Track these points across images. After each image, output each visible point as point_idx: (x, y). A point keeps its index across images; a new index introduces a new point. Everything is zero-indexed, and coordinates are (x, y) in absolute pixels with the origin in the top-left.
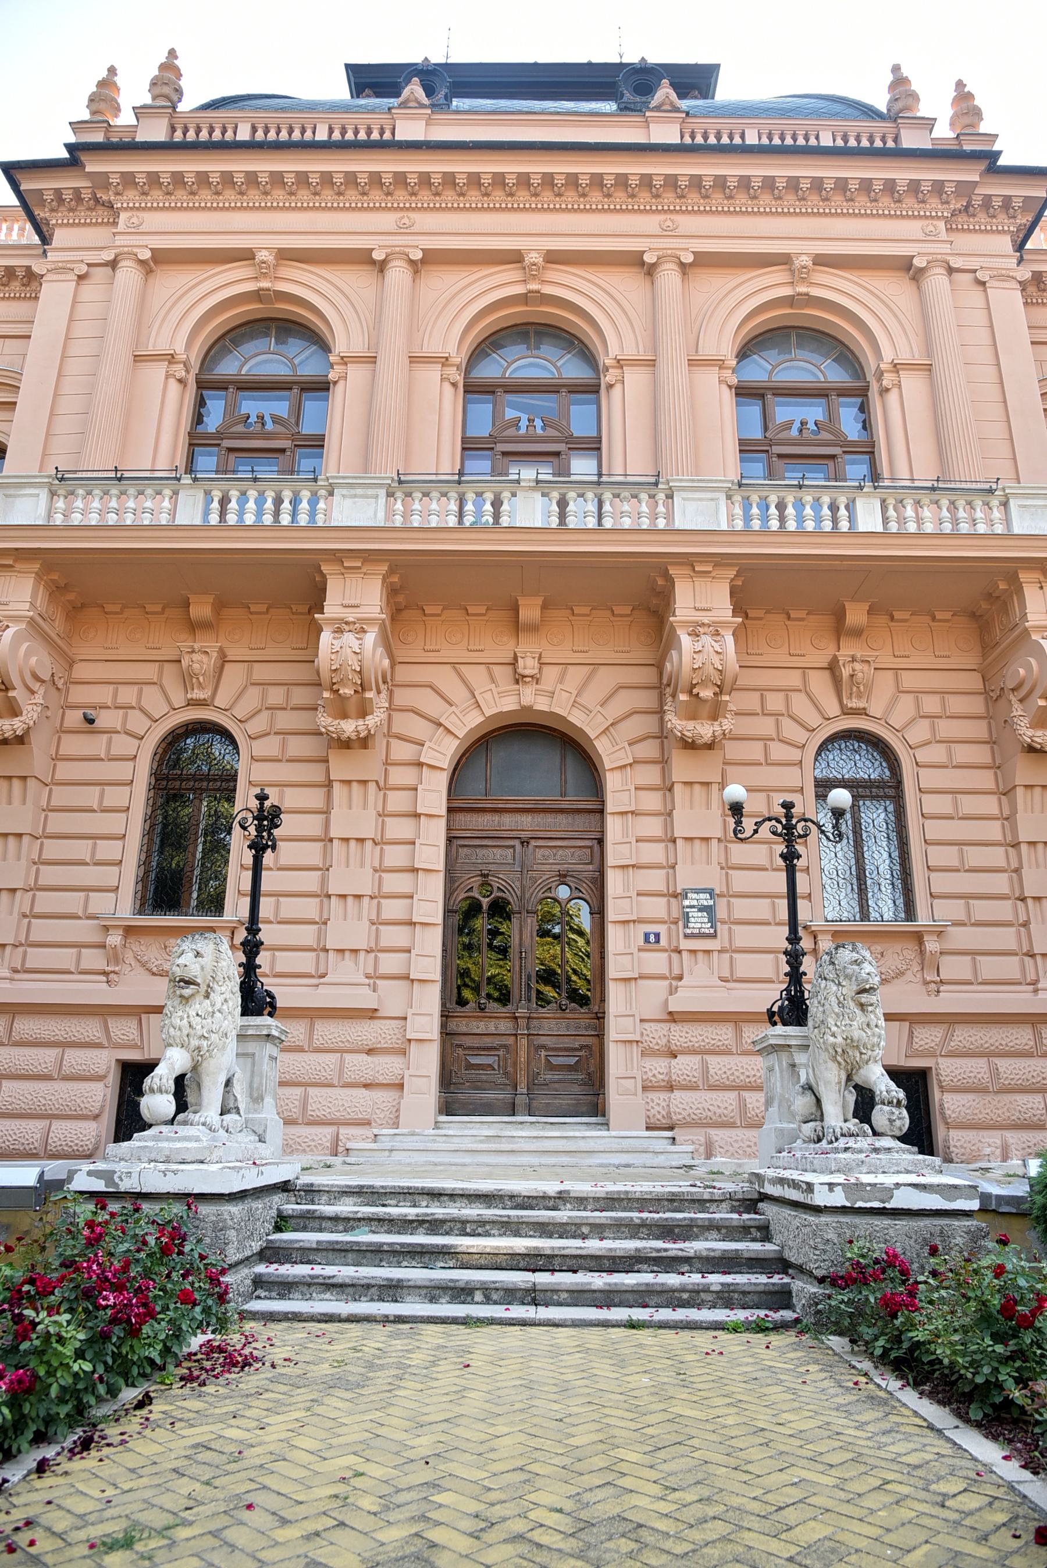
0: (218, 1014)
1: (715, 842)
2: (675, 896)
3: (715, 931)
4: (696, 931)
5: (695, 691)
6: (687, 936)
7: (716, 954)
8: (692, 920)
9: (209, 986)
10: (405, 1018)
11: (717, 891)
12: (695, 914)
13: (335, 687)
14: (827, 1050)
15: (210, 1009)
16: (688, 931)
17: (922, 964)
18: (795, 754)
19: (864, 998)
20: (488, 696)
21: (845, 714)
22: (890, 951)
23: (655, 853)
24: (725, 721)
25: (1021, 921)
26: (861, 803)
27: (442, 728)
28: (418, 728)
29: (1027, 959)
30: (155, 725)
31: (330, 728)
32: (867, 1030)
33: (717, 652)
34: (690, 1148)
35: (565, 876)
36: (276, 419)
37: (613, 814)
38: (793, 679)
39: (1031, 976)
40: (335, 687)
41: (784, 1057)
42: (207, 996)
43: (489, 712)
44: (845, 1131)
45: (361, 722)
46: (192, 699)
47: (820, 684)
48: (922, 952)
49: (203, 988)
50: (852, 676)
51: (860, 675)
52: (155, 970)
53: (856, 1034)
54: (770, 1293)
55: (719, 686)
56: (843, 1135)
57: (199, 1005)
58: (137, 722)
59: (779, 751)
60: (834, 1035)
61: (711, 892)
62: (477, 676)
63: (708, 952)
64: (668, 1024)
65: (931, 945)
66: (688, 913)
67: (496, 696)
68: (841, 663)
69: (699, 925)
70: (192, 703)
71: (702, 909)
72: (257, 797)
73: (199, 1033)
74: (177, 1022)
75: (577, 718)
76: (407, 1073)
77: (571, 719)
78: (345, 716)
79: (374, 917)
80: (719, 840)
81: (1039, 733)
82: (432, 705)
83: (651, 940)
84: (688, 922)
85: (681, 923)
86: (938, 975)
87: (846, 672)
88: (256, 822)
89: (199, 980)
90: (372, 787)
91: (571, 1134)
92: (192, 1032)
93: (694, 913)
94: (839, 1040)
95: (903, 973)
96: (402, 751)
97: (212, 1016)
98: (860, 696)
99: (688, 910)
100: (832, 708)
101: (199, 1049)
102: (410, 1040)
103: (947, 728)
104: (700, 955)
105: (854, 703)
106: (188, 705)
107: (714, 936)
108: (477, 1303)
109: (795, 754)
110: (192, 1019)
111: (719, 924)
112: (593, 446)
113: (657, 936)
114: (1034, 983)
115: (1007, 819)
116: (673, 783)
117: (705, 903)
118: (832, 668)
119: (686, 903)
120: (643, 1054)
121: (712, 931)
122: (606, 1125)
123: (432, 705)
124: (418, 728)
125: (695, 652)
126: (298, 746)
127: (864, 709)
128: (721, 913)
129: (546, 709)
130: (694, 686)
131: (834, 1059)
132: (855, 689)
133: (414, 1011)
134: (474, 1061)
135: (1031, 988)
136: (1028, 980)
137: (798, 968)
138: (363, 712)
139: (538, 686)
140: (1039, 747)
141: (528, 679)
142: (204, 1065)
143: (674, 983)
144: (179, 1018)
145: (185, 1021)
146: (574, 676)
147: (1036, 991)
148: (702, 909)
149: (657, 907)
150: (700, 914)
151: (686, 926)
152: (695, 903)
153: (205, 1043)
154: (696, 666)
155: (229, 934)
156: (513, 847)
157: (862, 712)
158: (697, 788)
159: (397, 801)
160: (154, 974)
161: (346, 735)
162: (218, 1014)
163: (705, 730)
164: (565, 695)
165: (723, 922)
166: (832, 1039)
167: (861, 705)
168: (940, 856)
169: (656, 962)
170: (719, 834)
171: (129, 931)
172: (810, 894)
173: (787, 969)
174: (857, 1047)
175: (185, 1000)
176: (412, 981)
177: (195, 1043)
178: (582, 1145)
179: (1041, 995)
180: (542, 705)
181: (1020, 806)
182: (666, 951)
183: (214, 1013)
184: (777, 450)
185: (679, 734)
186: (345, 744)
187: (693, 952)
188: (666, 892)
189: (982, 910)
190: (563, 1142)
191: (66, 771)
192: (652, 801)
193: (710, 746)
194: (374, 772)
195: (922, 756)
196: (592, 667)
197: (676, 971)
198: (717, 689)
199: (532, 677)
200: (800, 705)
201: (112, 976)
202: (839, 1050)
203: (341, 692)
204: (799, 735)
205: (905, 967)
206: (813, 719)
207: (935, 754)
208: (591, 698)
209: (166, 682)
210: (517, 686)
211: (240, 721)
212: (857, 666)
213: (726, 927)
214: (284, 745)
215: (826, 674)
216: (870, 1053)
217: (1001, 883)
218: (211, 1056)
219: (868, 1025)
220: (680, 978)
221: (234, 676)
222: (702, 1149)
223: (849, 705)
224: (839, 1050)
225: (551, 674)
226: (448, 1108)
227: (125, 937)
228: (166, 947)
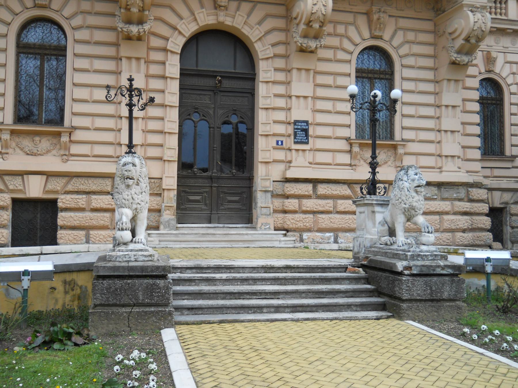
0: (144, 193)
1: (310, 99)
2: (289, 123)
3: (308, 141)
4: (299, 140)
5: (311, 24)
6: (295, 143)
7: (307, 152)
8: (298, 135)
9: (138, 180)
10: (161, 179)
11: (310, 122)
12: (299, 133)
13: (128, 7)
14: (401, 210)
15: (141, 191)
16: (296, 140)
17: (395, 157)
18: (347, 57)
19: (419, 189)
20: (201, 15)
21: (372, 38)
22: (382, 152)
23: (281, 103)
24: (322, 40)
25: (438, 141)
26: (374, 80)
27: (177, 32)
28: (164, 30)
29: (438, 158)
30: (16, 17)
31: (124, 29)
32: (419, 202)
33: (324, 5)
34: (294, 239)
35: (235, 110)
37: (262, 82)
38: (350, 18)
39: (439, 165)
40: (128, 7)
41: (370, 208)
42: (138, 184)
43: (201, 24)
44: (406, 242)
45: (140, 27)
46: (38, 4)
47: (362, 21)
48: (396, 154)
49: (136, 181)
50: (378, 19)
51: (382, 19)
52: (28, 152)
53: (414, 204)
54: (378, 305)
55: (322, 22)
56: (406, 244)
57: (135, 189)
59: (341, 55)
60: (405, 204)
61: (307, 122)
63: (304, 151)
64: (284, 183)
65: (401, 151)
66: (296, 132)
67: (205, 15)
68: (374, 11)
69: (301, 138)
70: (36, 6)
71: (303, 130)
72: (129, 80)
73: (137, 202)
74: (126, 197)
76: (164, 205)
77: (244, 31)
78: (129, 22)
79: (144, 128)
80: (312, 97)
81: (459, 56)
82: (172, 19)
83: (279, 145)
84: (296, 136)
85: (292, 137)
86: (402, 164)
87: (375, 17)
88: (129, 93)
89: (135, 177)
90: (142, 61)
91: (241, 232)
92: (134, 202)
93: (299, 133)
94: (407, 206)
95: (387, 162)
96: (155, 42)
97: (141, 194)
98: (380, 29)
99: (296, 130)
100: (366, 34)
101: (136, 209)
102: (164, 190)
103: (417, 49)
104: (300, 152)
105: (377, 33)
106: (34, 7)
107: (307, 143)
108: (264, 313)
109: (347, 57)
110: (133, 196)
111: (310, 138)
113: (282, 142)
114: (440, 168)
115: (437, 94)
116: (292, 69)
117: (304, 127)
118: (368, 14)
119: (296, 127)
120: (273, 196)
121: (307, 141)
122: (254, 228)
123: (172, 19)
124: (164, 30)
125: (313, 4)
126: (100, 36)
127: (381, 36)
128: (311, 132)
129: (230, 24)
130: (310, 22)
131: (404, 213)
132: (378, 26)
133: (166, 175)
134: (192, 198)
135: (438, 170)
136: (438, 167)
137: (375, 170)
139: (227, 12)
140: (458, 62)
141: (223, 8)
142: (139, 216)
143: (288, 164)
144: (127, 194)
145: (130, 197)
147: (441, 172)
148: (303, 130)
149: (281, 129)
150: (302, 133)
151: (295, 138)
152: (299, 127)
153: (139, 206)
154: (313, 12)
155: (68, 134)
156: (210, 95)
157: (380, 38)
158: (303, 72)
160: (28, 154)
161: (133, 34)
162: (144, 193)
163: (313, 44)
164: (240, 18)
165: (311, 137)
166: (404, 206)
167: (380, 34)
169: (280, 155)
170: (312, 95)
171: (13, 132)
172: (350, 125)
173: (370, 170)
174: (414, 209)
175: (128, 186)
176: (164, 161)
177: (135, 206)
178: (246, 238)
179: (444, 173)
180: (228, 21)
181: (445, 89)
182: (284, 149)
183: (142, 192)
185: (300, 45)
186: (129, 38)
187: (297, 150)
188: (286, 121)
189: (423, 135)
190: (238, 236)
192: (281, 77)
193: (312, 52)
194: (142, 54)
196: (253, 3)
197: (289, 159)
198: (321, 24)
199: (224, 7)
200: (352, 32)
201: (5, 156)
202: (407, 210)
203: (132, 10)
204: (350, 47)
205: (388, 160)
206: (357, 39)
207: (410, 61)
210: (216, 11)
211: (66, 18)
212: (382, 15)
213: (313, 139)
214: (92, 35)
215: (365, 17)
216: (418, 211)
217: (430, 124)
218: (141, 212)
219: (419, 200)
220: (290, 162)
222: (298, 240)
223: (375, 34)
224: (407, 210)
226: (180, 221)
227: (11, 135)
228: (33, 141)
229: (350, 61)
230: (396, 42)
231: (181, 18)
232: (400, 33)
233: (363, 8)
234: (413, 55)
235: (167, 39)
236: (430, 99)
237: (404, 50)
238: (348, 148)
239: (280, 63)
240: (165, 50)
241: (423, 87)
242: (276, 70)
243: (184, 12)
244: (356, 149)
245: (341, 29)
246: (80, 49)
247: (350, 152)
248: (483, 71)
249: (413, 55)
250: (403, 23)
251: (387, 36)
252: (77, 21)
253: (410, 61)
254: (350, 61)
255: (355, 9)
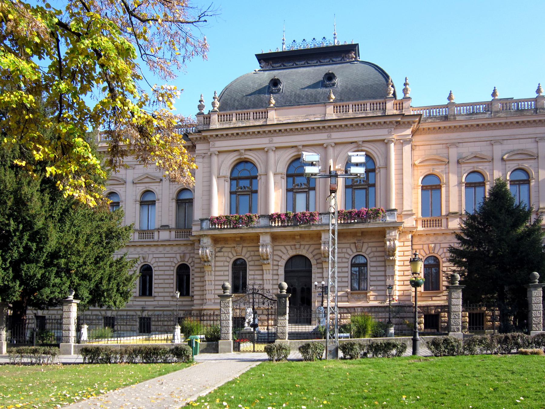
18: (347, 260)
28: (277, 258)
36: (248, 187)
38: (348, 245)
47: (353, 246)
58: (228, 259)
59: (344, 260)
62: (288, 248)
75: (307, 255)
96: (275, 263)
100: (355, 250)
103: (376, 254)
109: (347, 260)
112: (314, 189)
118: (355, 243)
124: (277, 258)
126: (257, 263)
138: (268, 259)
146: (307, 247)
159: (275, 272)
168: (372, 279)
180: (300, 253)
184: (354, 187)
191: (217, 269)
192: (320, 271)
195: (372, 260)
200: (349, 251)
206: (351, 253)
207: (374, 259)
208: (311, 250)
209: (233, 252)
221: (245, 250)
225: (302, 247)
229: (348, 262)
230: (368, 252)
231: (284, 254)
232: (370, 249)
233: (353, 241)
234: (375, 257)
235: (279, 261)
236: (383, 273)
237: (370, 256)
238: (346, 295)
239: (319, 266)
240: (278, 265)
241: (379, 269)
242: (318, 268)
243: (285, 251)
244: (349, 296)
245: (344, 250)
246: (251, 268)
247: (347, 296)
248: (428, 252)
249: (375, 257)
250: (370, 244)
251: (363, 250)
252: (250, 259)
253: (374, 259)
254: (348, 262)
255: (349, 242)
